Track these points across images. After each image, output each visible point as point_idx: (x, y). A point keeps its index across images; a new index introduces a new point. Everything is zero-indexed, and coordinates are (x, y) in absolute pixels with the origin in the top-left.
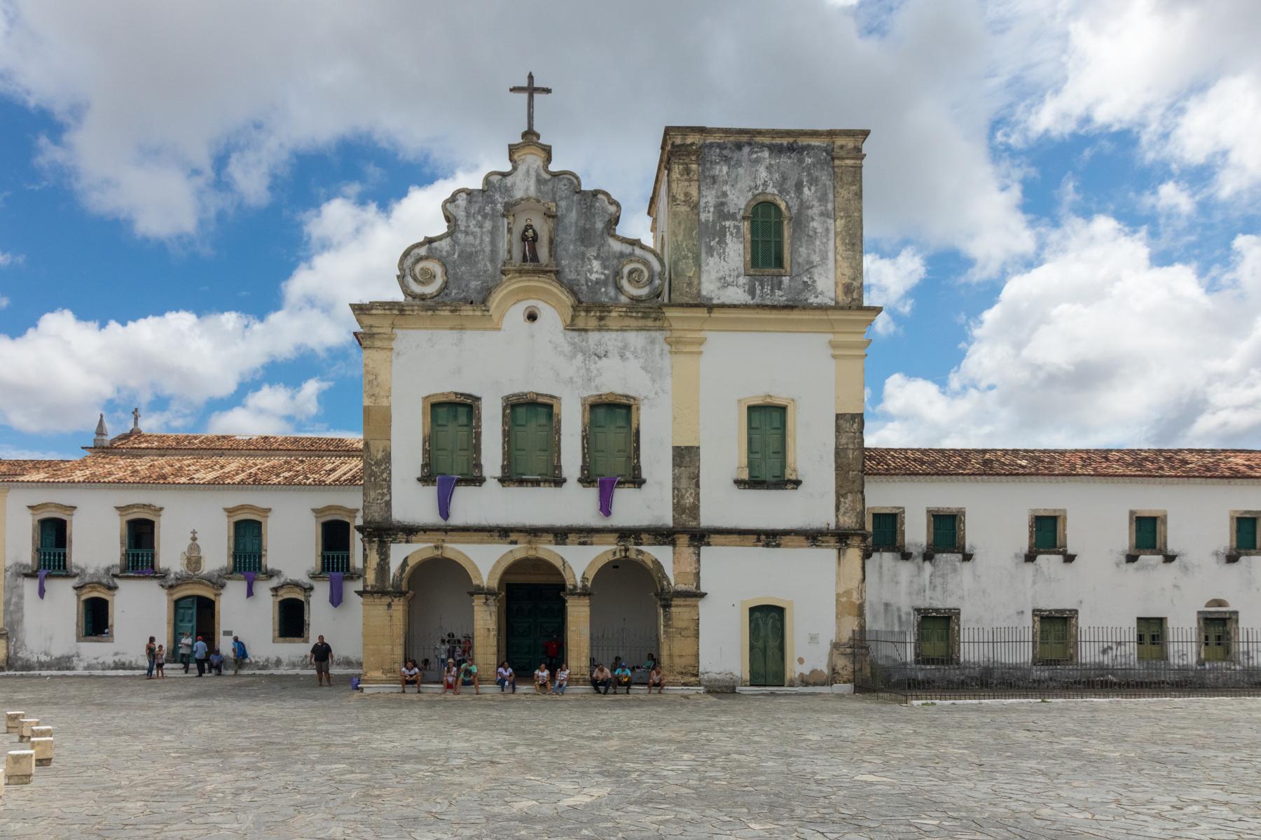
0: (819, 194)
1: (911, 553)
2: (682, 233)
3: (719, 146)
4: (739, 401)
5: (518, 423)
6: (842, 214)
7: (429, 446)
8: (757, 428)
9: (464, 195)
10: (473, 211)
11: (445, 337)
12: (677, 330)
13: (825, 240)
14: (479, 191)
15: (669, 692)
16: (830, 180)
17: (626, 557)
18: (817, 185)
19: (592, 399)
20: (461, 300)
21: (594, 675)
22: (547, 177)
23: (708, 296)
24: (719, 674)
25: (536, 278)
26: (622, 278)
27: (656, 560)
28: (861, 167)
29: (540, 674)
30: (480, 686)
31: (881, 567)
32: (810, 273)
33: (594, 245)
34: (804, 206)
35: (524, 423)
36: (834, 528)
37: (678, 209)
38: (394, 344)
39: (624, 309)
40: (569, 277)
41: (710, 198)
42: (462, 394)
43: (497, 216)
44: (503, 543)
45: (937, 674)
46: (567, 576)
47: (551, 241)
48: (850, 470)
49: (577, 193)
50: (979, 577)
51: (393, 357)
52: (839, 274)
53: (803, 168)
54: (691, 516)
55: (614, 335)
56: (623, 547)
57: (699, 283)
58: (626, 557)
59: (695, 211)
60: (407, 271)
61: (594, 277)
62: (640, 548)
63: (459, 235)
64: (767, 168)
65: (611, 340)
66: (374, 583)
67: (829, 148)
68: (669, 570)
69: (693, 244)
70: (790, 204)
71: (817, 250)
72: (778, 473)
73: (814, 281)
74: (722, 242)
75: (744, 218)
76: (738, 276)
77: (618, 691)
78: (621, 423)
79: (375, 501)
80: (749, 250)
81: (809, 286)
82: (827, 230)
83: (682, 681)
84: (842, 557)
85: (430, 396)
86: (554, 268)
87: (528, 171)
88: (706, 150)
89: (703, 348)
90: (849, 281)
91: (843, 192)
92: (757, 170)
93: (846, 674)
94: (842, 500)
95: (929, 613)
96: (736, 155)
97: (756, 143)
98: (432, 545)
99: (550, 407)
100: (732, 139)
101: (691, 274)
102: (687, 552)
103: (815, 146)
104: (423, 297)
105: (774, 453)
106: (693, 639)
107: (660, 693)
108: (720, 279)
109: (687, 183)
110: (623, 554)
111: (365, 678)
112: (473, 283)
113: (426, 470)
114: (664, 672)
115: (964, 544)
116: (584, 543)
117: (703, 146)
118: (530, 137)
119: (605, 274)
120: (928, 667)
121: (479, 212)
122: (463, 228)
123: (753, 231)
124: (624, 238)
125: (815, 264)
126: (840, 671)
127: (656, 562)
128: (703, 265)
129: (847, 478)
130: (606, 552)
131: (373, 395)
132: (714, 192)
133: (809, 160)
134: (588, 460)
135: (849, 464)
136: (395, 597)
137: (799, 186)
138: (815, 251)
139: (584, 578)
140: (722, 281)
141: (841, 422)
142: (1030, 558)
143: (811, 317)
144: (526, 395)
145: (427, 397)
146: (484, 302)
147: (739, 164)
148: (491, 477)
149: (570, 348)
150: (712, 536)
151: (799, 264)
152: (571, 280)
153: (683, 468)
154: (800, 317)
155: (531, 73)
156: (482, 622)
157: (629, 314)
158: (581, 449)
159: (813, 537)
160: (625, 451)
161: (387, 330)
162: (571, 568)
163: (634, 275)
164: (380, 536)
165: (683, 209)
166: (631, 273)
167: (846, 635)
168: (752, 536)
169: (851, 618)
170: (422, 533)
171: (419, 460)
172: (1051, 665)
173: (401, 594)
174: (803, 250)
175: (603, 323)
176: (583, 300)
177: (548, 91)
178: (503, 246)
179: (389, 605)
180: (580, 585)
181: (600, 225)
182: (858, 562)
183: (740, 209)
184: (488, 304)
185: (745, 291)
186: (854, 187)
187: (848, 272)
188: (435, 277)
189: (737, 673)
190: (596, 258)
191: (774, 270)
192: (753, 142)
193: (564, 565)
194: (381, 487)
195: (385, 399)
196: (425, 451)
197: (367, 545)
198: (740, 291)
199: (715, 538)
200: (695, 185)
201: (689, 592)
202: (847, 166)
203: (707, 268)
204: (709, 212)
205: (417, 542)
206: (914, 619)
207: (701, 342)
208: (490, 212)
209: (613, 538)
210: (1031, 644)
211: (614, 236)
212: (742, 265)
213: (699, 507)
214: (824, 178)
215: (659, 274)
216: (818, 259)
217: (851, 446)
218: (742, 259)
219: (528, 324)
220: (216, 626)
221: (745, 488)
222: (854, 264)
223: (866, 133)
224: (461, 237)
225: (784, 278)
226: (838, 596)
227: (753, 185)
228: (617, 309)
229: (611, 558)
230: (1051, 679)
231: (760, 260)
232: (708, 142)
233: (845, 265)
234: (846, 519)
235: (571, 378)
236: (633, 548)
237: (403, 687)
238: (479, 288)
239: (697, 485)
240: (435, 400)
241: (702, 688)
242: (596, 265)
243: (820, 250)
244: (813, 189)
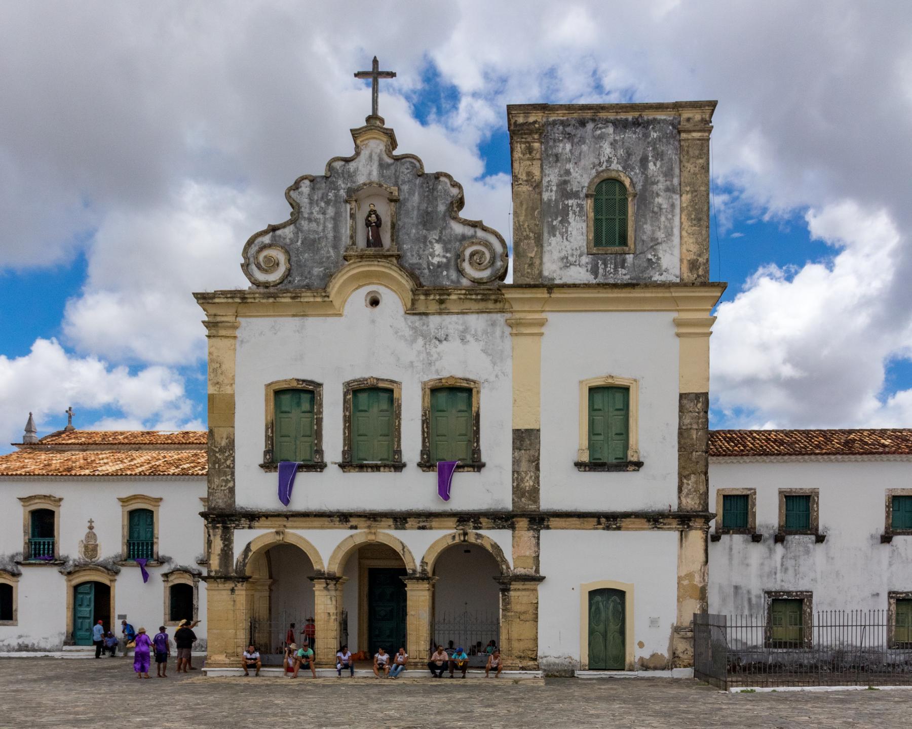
0: (664, 169)
1: (761, 535)
2: (523, 212)
3: (562, 123)
4: (581, 382)
5: (361, 408)
6: (688, 189)
7: (272, 432)
8: (600, 410)
9: (307, 182)
10: (316, 198)
11: (288, 325)
12: (518, 311)
13: (670, 216)
14: (323, 177)
15: (506, 676)
16: (676, 154)
17: (464, 541)
18: (662, 160)
19: (432, 383)
20: (303, 287)
21: (433, 658)
22: (390, 161)
23: (550, 277)
24: (558, 658)
25: (376, 263)
26: (464, 260)
27: (495, 543)
28: (708, 140)
29: (380, 657)
30: (316, 670)
31: (731, 549)
32: (655, 250)
33: (435, 228)
34: (649, 181)
35: (365, 408)
36: (676, 510)
37: (520, 189)
38: (238, 333)
39: (463, 292)
40: (411, 262)
41: (552, 177)
42: (304, 381)
43: (340, 202)
44: (345, 528)
46: (407, 560)
47: (393, 226)
48: (693, 450)
49: (419, 176)
50: (832, 558)
51: (237, 346)
52: (684, 251)
53: (649, 143)
54: (530, 499)
55: (454, 318)
56: (462, 531)
57: (541, 264)
58: (464, 541)
59: (537, 190)
60: (252, 259)
61: (436, 260)
63: (303, 222)
64: (611, 144)
65: (452, 323)
66: (218, 569)
67: (676, 122)
68: (508, 555)
69: (535, 224)
70: (635, 180)
71: (662, 227)
72: (621, 456)
73: (659, 259)
74: (565, 221)
75: (587, 196)
76: (580, 256)
77: (454, 675)
78: (462, 406)
79: (219, 488)
80: (593, 229)
81: (654, 263)
82: (673, 206)
83: (520, 666)
84: (684, 539)
85: (272, 383)
86: (396, 253)
87: (371, 157)
88: (549, 128)
89: (543, 330)
90: (695, 257)
91: (690, 166)
92: (601, 147)
93: (687, 657)
94: (685, 481)
96: (580, 132)
97: (600, 118)
98: (274, 530)
99: (391, 391)
101: (532, 255)
102: (526, 535)
103: (661, 120)
104: (266, 285)
105: (617, 434)
106: (532, 622)
107: (496, 677)
108: (562, 259)
109: (529, 163)
110: (462, 538)
111: (209, 661)
112: (316, 269)
113: (268, 457)
114: (503, 656)
115: (818, 525)
116: (423, 528)
117: (547, 124)
118: (373, 121)
119: (447, 258)
120: (780, 650)
121: (322, 198)
122: (306, 216)
123: (597, 209)
124: (466, 220)
125: (660, 240)
126: (681, 655)
127: (496, 546)
128: (545, 245)
129: (690, 459)
130: (445, 536)
131: (218, 383)
132: (556, 171)
133: (654, 135)
134: (428, 444)
135: (693, 445)
136: (238, 582)
137: (644, 161)
138: (659, 228)
139: (423, 563)
140: (565, 261)
141: (685, 401)
142: (886, 539)
143: (653, 295)
144: (367, 380)
145: (270, 385)
146: (325, 289)
147: (582, 141)
148: (332, 463)
149: (411, 333)
150: (552, 519)
151: (643, 241)
152: (413, 264)
153: (523, 451)
154: (642, 295)
155: (375, 57)
156: (322, 607)
157: (469, 297)
158: (420, 433)
160: (466, 435)
162: (410, 553)
163: (475, 257)
164: (224, 522)
165: (525, 188)
166: (472, 255)
167: (688, 619)
168: (591, 519)
169: (693, 601)
170: (264, 518)
171: (262, 448)
172: (907, 648)
173: (242, 578)
174: (648, 227)
175: (443, 306)
176: (424, 284)
177: (392, 75)
178: (345, 232)
179: (233, 590)
180: (419, 569)
181: (442, 208)
182: (701, 545)
183: (583, 188)
184: (328, 290)
185: (587, 270)
186: (701, 161)
187: (694, 248)
188: (278, 264)
189: (576, 657)
190: (438, 241)
191: (617, 248)
192: (597, 118)
193: (403, 549)
194: (225, 474)
195: (228, 387)
196: (269, 439)
197: (211, 531)
198: (583, 271)
199: (554, 522)
200: (537, 164)
201: (529, 576)
203: (549, 248)
204: (551, 191)
205: (259, 527)
206: (764, 602)
207: (542, 323)
208: (333, 198)
209: (452, 522)
210: (885, 628)
211: (456, 219)
212: (585, 244)
213: (539, 490)
214: (670, 152)
215: (501, 256)
216: (663, 236)
217: (695, 426)
218: (585, 238)
219: (369, 310)
220: (112, 610)
221: (585, 471)
222: (700, 240)
223: (713, 105)
224: (304, 224)
225: (627, 256)
226: (680, 579)
227: (597, 162)
228: (456, 292)
229: (450, 542)
230: (906, 663)
231: (604, 238)
232: (551, 119)
233: (691, 241)
234: (689, 500)
235: (412, 363)
236: (472, 532)
237: (246, 670)
238: (322, 274)
239: (537, 468)
240: (277, 387)
241: (540, 672)
242: (438, 248)
243: (666, 227)
244: (658, 164)
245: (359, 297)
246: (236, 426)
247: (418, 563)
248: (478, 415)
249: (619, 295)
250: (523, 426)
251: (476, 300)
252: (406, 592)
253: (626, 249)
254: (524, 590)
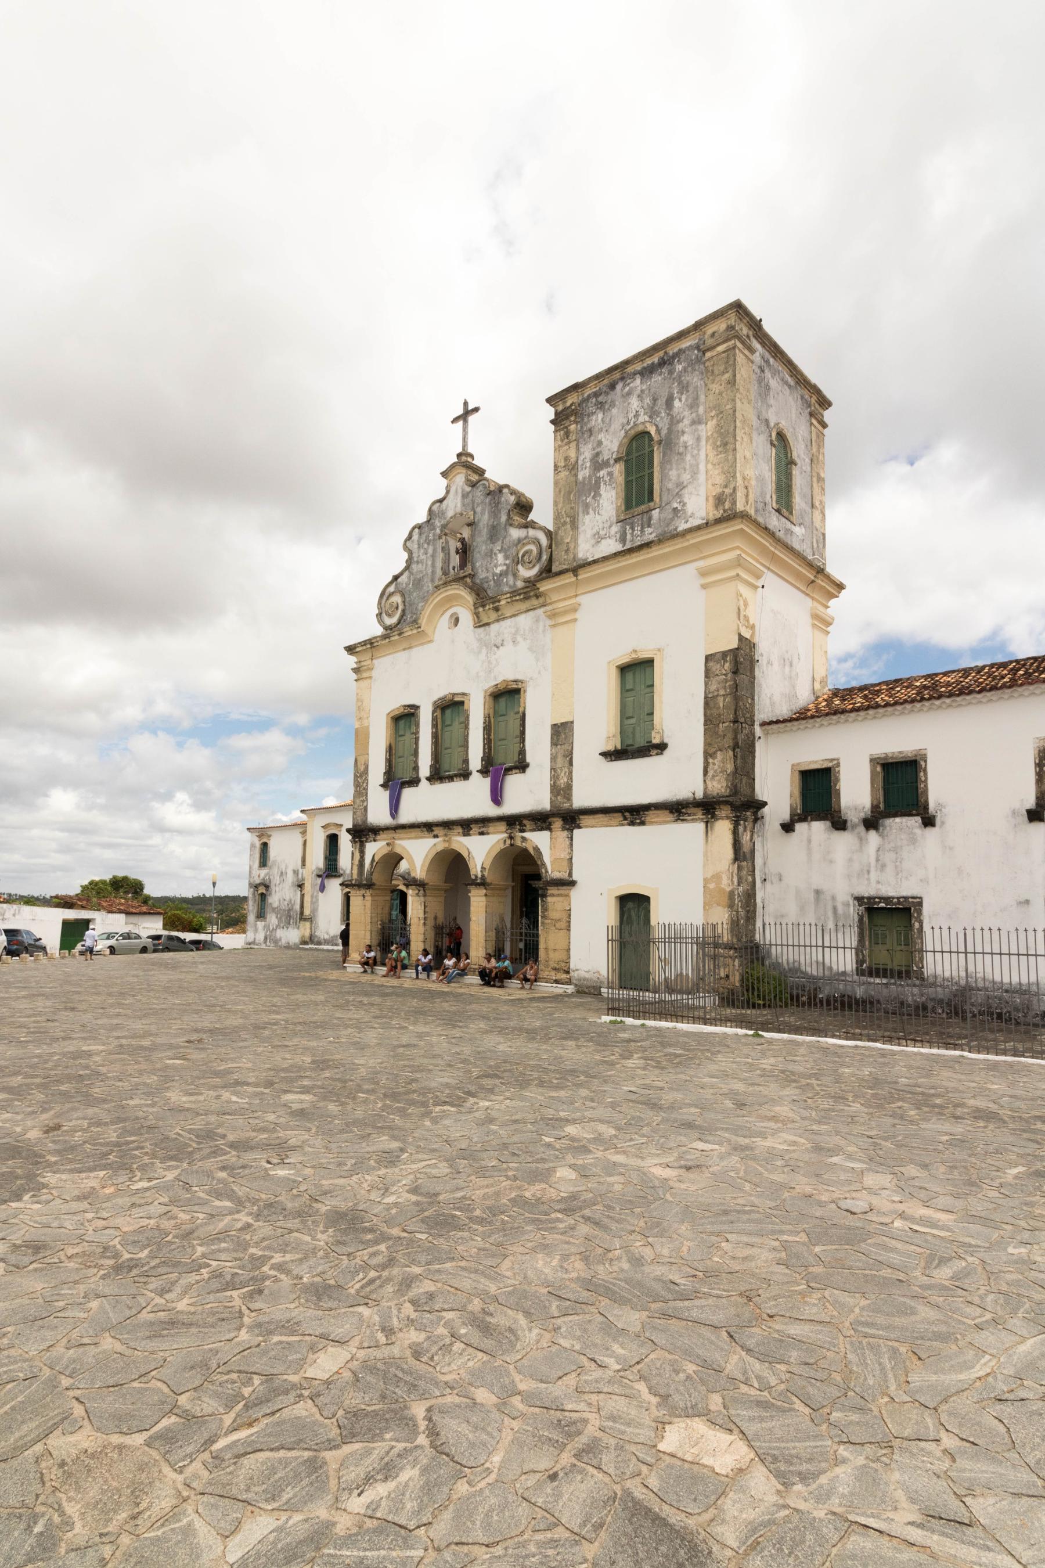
0: (690, 401)
4: (609, 663)
6: (713, 414)
8: (632, 690)
9: (417, 530)
11: (401, 657)
13: (696, 452)
33: (498, 539)
41: (587, 453)
45: (885, 991)
46: (471, 866)
52: (710, 486)
58: (512, 845)
61: (498, 571)
62: (524, 834)
68: (547, 858)
70: (660, 426)
71: (688, 467)
74: (597, 495)
75: (616, 461)
76: (610, 527)
81: (679, 511)
89: (577, 615)
91: (715, 387)
94: (711, 760)
95: (875, 903)
100: (606, 382)
101: (568, 540)
102: (562, 835)
123: (628, 472)
127: (537, 849)
129: (717, 733)
135: (719, 715)
137: (669, 403)
139: (483, 868)
141: (711, 664)
147: (613, 404)
154: (661, 552)
159: (678, 809)
161: (369, 662)
164: (360, 837)
165: (564, 474)
168: (616, 815)
173: (369, 886)
174: (673, 474)
180: (479, 875)
187: (719, 480)
190: (500, 551)
199: (585, 820)
200: (573, 445)
202: (719, 354)
207: (575, 610)
209: (502, 826)
216: (689, 477)
217: (722, 692)
226: (706, 881)
227: (625, 421)
229: (502, 846)
232: (586, 395)
233: (716, 472)
234: (715, 784)
239: (571, 763)
242: (500, 557)
243: (691, 466)
244: (684, 398)
245: (445, 620)
246: (370, 753)
247: (479, 869)
248: (524, 715)
249: (639, 559)
250: (558, 721)
251: (520, 600)
252: (469, 898)
253: (652, 504)
254: (558, 895)
